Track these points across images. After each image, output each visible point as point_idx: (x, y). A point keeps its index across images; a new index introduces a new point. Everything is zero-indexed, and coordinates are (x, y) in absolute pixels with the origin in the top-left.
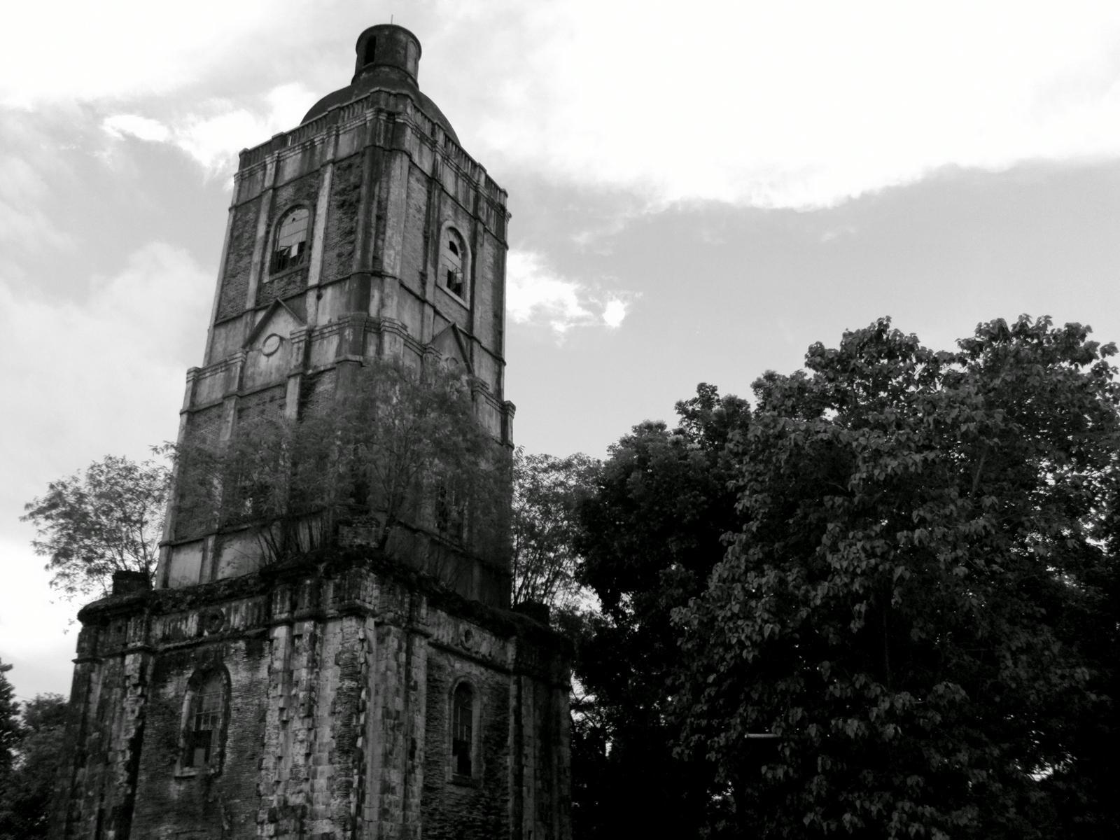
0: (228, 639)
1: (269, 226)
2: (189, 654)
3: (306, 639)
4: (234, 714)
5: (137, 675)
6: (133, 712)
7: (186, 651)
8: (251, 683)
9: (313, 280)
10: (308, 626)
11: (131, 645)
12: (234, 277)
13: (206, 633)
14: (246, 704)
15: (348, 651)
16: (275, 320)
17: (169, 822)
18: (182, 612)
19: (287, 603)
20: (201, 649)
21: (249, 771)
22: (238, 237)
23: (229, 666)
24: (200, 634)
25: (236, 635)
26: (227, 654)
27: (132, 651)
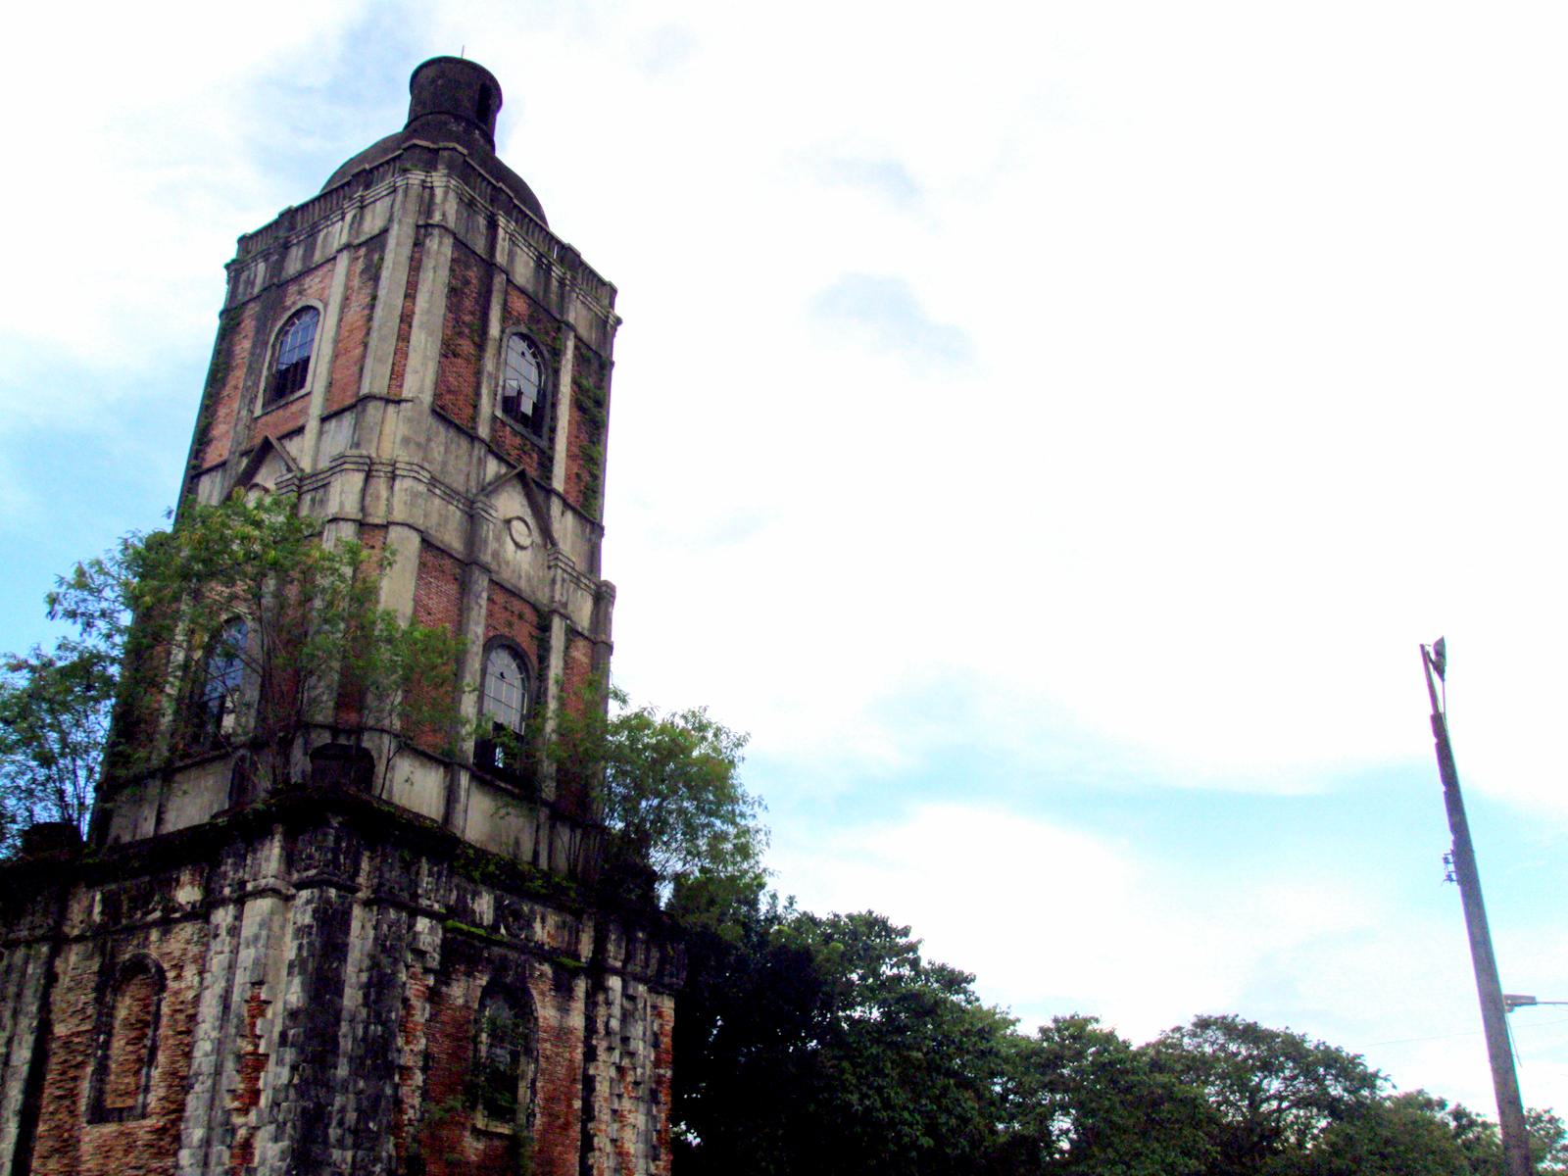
0: (534, 955)
2: (482, 950)
7: (477, 943)
8: (561, 1028)
11: (424, 902)
12: (455, 356)
14: (557, 1054)
18: (471, 880)
19: (623, 951)
20: (496, 950)
21: (563, 1145)
23: (534, 993)
24: (495, 928)
25: (541, 953)
26: (531, 975)
27: (429, 914)
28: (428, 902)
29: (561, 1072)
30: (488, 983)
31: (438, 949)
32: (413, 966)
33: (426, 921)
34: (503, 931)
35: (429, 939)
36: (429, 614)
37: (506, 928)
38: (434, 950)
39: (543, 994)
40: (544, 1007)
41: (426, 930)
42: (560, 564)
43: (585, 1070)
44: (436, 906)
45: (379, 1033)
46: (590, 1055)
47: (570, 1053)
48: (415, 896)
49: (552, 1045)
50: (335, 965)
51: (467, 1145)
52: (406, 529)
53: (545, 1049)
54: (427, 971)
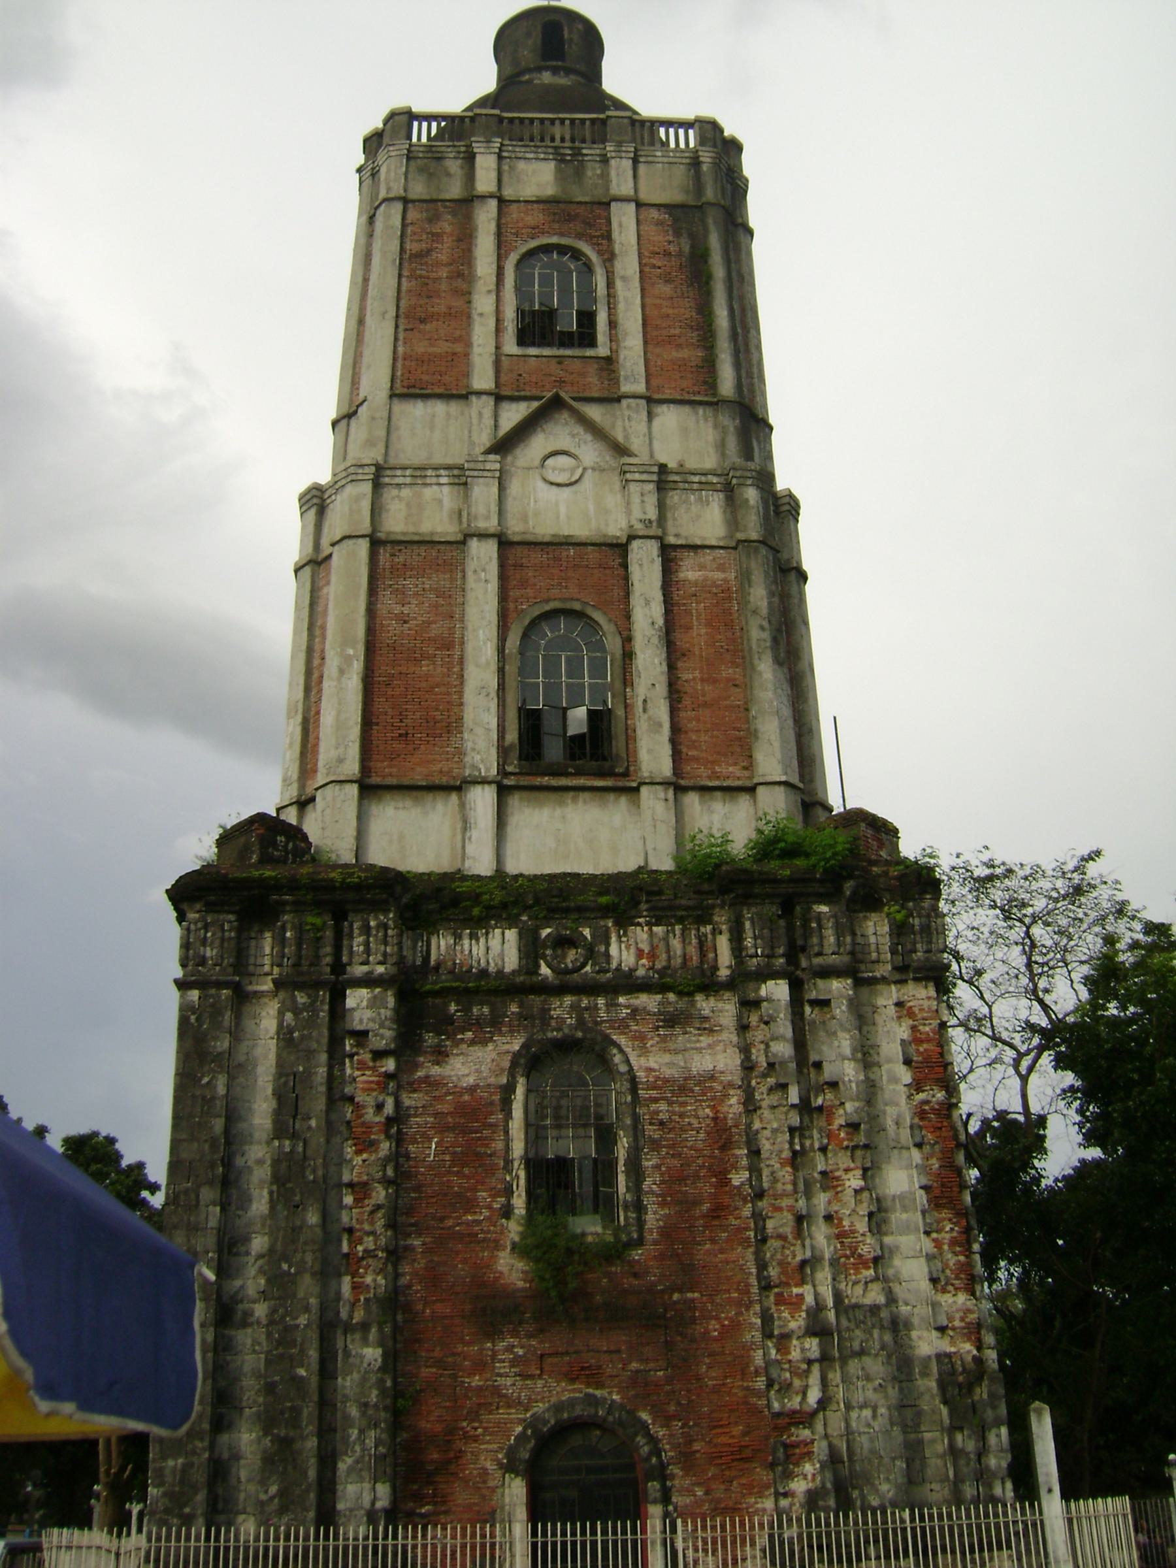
1: (500, 258)
3: (840, 1010)
4: (651, 1131)
5: (389, 1034)
6: (380, 1107)
9: (633, 379)
10: (838, 987)
12: (423, 321)
13: (545, 970)
15: (928, 1040)
16: (549, 426)
17: (515, 1334)
21: (713, 1241)
22: (418, 256)
23: (622, 1040)
27: (368, 981)
28: (365, 968)
29: (697, 1138)
30: (523, 1046)
31: (387, 1023)
32: (357, 1054)
33: (364, 992)
34: (545, 970)
35: (369, 1014)
36: (405, 622)
37: (549, 966)
38: (382, 1026)
39: (641, 1038)
40: (644, 1051)
41: (365, 1003)
42: (628, 476)
43: (749, 1126)
44: (381, 969)
45: (287, 1149)
46: (750, 1106)
47: (713, 1107)
48: (338, 967)
49: (670, 1103)
50: (205, 1080)
51: (505, 1270)
52: (351, 542)
53: (657, 1112)
54: (378, 1055)
